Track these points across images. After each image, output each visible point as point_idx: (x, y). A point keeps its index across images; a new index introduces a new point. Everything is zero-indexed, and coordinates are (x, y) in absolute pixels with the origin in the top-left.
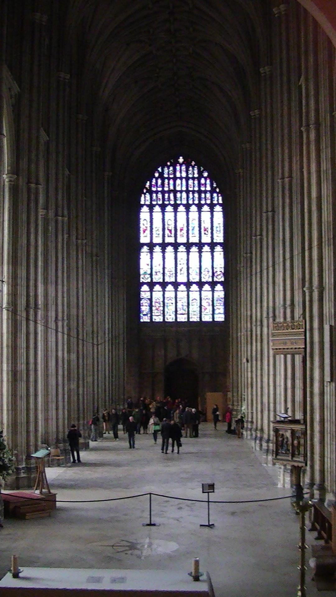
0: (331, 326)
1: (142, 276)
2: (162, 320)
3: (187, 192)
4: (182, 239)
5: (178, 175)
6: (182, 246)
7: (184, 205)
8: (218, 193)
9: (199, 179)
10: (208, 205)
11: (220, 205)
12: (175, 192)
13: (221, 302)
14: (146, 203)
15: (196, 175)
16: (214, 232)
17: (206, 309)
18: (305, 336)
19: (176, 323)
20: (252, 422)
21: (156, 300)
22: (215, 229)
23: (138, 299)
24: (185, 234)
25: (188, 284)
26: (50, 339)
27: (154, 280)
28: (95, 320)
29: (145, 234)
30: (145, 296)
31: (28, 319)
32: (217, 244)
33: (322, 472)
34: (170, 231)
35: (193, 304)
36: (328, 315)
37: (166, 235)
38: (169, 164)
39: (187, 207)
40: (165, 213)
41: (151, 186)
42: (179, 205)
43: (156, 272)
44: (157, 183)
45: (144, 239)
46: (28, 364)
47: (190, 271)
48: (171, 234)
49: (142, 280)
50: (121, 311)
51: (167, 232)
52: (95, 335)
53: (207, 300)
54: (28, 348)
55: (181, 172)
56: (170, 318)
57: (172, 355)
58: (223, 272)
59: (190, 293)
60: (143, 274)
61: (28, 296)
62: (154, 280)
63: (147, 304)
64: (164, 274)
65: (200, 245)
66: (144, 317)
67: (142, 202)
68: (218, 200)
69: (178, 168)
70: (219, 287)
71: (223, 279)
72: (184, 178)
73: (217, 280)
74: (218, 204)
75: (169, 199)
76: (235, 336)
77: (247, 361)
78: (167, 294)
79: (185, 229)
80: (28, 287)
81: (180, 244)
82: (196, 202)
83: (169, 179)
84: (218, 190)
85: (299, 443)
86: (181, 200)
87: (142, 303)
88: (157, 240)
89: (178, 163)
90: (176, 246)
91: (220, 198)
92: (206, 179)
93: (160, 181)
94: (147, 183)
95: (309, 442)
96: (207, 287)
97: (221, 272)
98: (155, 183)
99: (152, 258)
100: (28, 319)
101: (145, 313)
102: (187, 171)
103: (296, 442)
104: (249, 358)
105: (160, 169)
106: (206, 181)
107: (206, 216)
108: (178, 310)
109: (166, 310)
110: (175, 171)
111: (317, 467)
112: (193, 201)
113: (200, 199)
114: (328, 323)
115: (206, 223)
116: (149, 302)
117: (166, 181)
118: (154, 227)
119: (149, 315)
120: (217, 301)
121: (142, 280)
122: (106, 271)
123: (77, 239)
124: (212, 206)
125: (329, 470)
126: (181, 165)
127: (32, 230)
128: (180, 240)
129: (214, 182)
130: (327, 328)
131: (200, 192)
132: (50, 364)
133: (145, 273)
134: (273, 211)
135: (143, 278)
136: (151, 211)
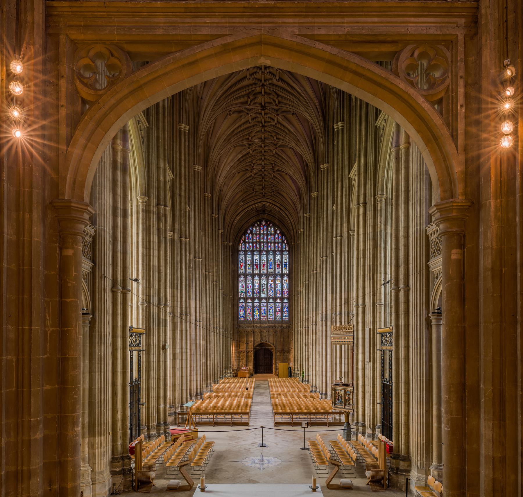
0: (370, 329)
3: (267, 243)
4: (264, 272)
5: (262, 232)
6: (264, 276)
8: (285, 244)
9: (274, 235)
11: (287, 251)
12: (260, 243)
15: (273, 233)
17: (278, 313)
18: (354, 334)
20: (308, 381)
25: (267, 299)
26: (192, 333)
28: (215, 321)
29: (242, 269)
31: (181, 322)
33: (364, 415)
34: (257, 267)
36: (368, 322)
38: (256, 225)
39: (267, 252)
41: (245, 239)
44: (249, 237)
45: (241, 271)
46: (182, 348)
49: (240, 296)
50: (228, 315)
51: (255, 267)
52: (215, 329)
54: (182, 339)
55: (263, 231)
57: (258, 341)
61: (181, 308)
64: (253, 292)
65: (275, 276)
69: (262, 228)
70: (286, 301)
75: (256, 248)
76: (296, 329)
77: (306, 345)
78: (255, 304)
79: (266, 265)
80: (181, 302)
81: (262, 275)
83: (256, 234)
84: (285, 242)
85: (349, 398)
86: (263, 248)
88: (249, 272)
89: (262, 224)
90: (260, 276)
92: (278, 235)
95: (355, 398)
96: (278, 301)
98: (248, 238)
99: (246, 283)
100: (181, 322)
102: (267, 230)
103: (347, 397)
104: (307, 344)
105: (251, 228)
106: (278, 236)
107: (278, 257)
110: (260, 229)
111: (360, 413)
112: (271, 248)
113: (275, 247)
114: (368, 327)
115: (278, 261)
121: (240, 296)
122: (221, 291)
123: (206, 272)
124: (282, 252)
125: (368, 415)
126: (263, 226)
127: (184, 267)
130: (367, 330)
131: (275, 243)
132: (192, 348)
134: (327, 256)
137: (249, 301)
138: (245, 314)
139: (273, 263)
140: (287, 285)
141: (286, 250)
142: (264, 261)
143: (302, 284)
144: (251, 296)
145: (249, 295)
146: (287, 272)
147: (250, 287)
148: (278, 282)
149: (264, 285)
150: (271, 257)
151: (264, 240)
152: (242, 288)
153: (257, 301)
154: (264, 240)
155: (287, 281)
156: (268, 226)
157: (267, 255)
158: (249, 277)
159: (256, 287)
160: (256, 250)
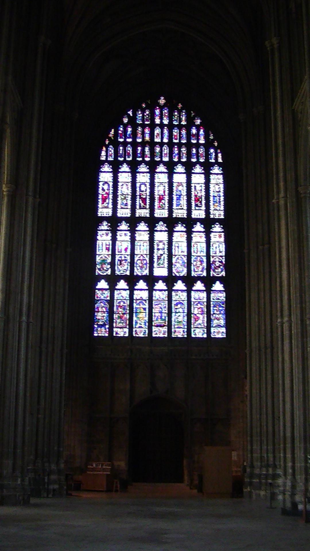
1: (98, 266)
2: (127, 335)
3: (171, 145)
4: (161, 213)
5: (158, 121)
6: (161, 223)
7: (165, 164)
9: (188, 128)
10: (201, 164)
11: (219, 165)
12: (152, 144)
13: (221, 308)
14: (109, 159)
15: (184, 123)
16: (211, 203)
17: (198, 318)
19: (150, 339)
21: (119, 303)
22: (211, 199)
23: (92, 301)
24: (167, 205)
27: (117, 273)
29: (105, 204)
30: (102, 297)
32: (215, 221)
34: (144, 200)
35: (178, 311)
37: (138, 207)
40: (138, 174)
41: (116, 134)
42: (158, 163)
44: (125, 131)
47: (174, 260)
48: (145, 204)
51: (138, 201)
53: (199, 306)
55: (161, 119)
56: (141, 332)
58: (224, 261)
59: (173, 294)
60: (101, 263)
62: (117, 273)
63: (104, 310)
66: (99, 329)
67: (103, 158)
68: (216, 158)
69: (157, 112)
70: (218, 286)
71: (223, 273)
72: (166, 125)
73: (215, 275)
74: (217, 163)
75: (143, 155)
78: (137, 295)
79: (167, 198)
82: (184, 160)
83: (144, 126)
84: (216, 144)
86: (161, 157)
87: (98, 308)
88: (124, 212)
89: (158, 104)
91: (220, 155)
92: (198, 128)
93: (130, 130)
94: (111, 131)
96: (199, 285)
97: (221, 262)
99: (114, 239)
101: (101, 323)
105: (130, 113)
106: (198, 131)
107: (198, 179)
108: (154, 319)
109: (135, 318)
110: (152, 116)
112: (180, 158)
113: (189, 155)
115: (199, 190)
116: (108, 306)
117: (140, 129)
118: (119, 193)
119: (107, 326)
120: (214, 306)
126: (162, 108)
128: (158, 213)
129: (210, 133)
131: (189, 146)
133: (103, 262)
135: (99, 269)
136: (116, 173)
137: (122, 284)
138: (111, 320)
139: (184, 193)
140: (223, 247)
141: (217, 163)
142: (161, 188)
143: (282, 184)
144: (128, 273)
145: (123, 269)
146: (220, 215)
147: (126, 250)
148: (199, 238)
149: (161, 246)
150: (180, 178)
151: (162, 138)
152: (105, 252)
153: (142, 284)
155: (220, 236)
156: (171, 107)
157: (171, 174)
158: (124, 226)
159: (142, 249)
160: (143, 161)
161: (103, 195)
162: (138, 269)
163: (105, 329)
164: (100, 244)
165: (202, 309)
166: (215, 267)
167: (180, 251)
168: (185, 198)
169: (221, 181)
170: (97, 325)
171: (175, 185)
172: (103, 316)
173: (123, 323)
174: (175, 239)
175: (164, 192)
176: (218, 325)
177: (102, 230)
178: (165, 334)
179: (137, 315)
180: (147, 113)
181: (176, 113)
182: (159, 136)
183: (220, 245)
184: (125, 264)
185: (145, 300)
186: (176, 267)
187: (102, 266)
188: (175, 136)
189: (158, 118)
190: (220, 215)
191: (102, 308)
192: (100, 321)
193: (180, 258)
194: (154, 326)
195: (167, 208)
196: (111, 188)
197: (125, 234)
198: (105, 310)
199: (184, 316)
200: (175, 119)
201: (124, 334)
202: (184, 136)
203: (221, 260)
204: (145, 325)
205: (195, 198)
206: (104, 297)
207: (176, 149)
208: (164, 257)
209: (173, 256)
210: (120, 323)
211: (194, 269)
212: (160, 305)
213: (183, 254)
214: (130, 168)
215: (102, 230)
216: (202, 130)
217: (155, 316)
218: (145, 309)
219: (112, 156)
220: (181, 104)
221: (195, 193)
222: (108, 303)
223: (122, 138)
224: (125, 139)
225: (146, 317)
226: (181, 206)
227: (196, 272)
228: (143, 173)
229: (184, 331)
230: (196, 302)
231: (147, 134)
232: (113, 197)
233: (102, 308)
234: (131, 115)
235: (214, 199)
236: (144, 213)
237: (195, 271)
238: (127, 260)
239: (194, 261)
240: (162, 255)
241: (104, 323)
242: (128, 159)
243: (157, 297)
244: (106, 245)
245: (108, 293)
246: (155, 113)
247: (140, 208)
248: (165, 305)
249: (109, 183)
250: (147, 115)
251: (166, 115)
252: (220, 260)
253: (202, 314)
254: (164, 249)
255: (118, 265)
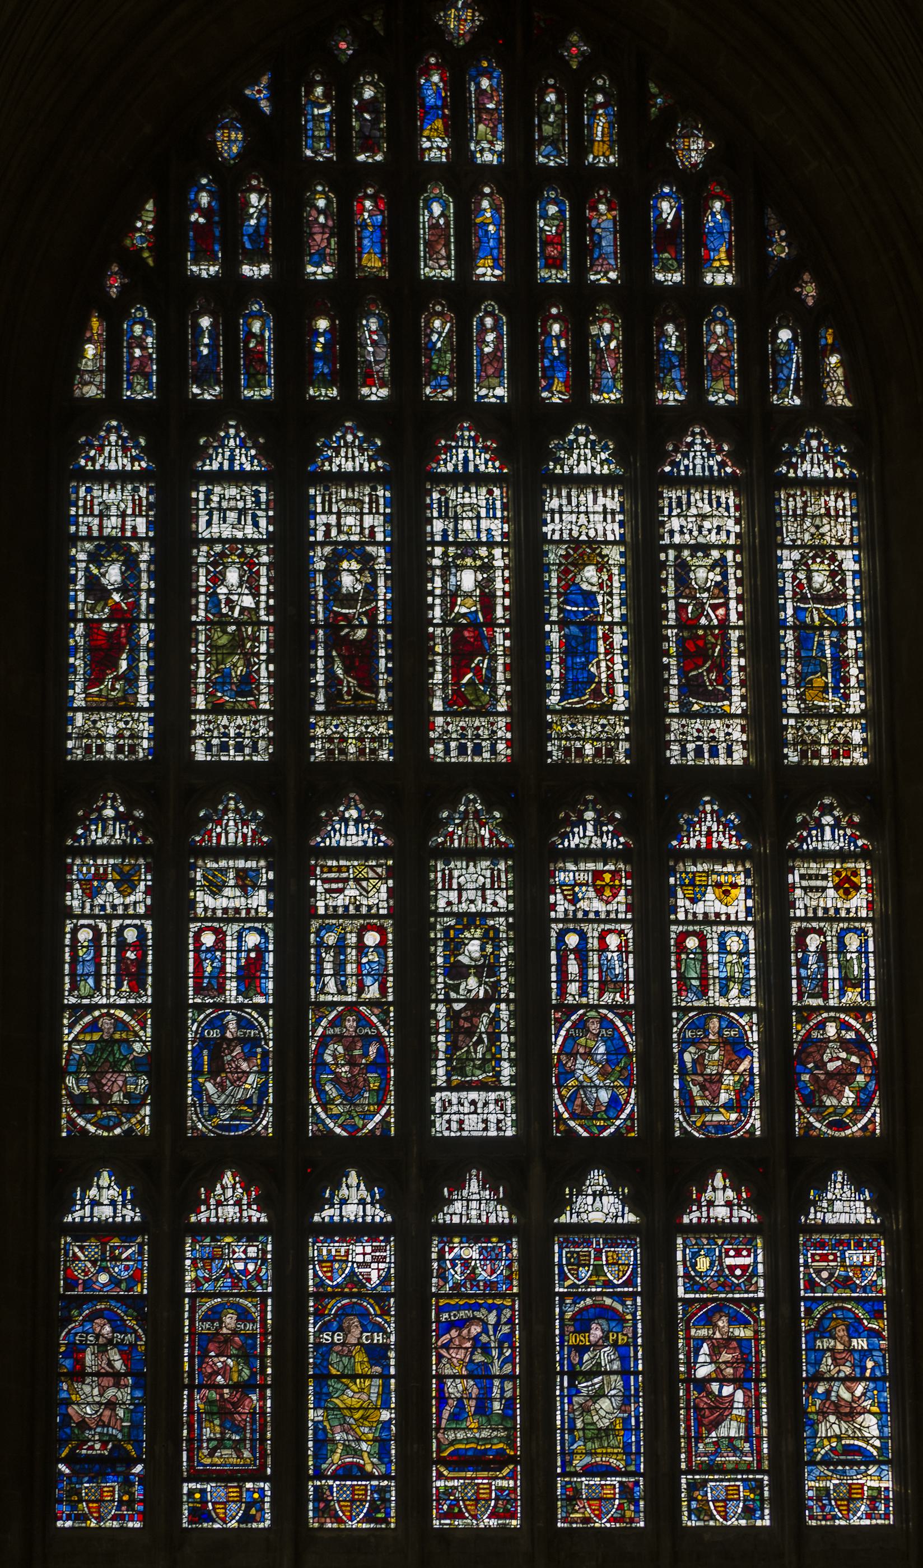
13: (860, 1343)
27: (198, 1123)
29: (111, 687)
43: (217, 1048)
59: (559, 1254)
62: (198, 1123)
84: (810, 291)
86: (463, 379)
87: (76, 1351)
97: (860, 1045)
116: (137, 1336)
120: (821, 1330)
135: (81, 1104)
142: (468, 580)
151: (466, 260)
154: (466, 260)
161: (91, 626)
162: (325, 1103)
163: (127, 1484)
164: (85, 935)
165: (740, 1346)
166: (815, 1078)
167: (593, 974)
168: (618, 640)
169: (843, 530)
170: (67, 1461)
171: (553, 556)
172: (111, 1405)
173: (237, 1447)
174: (561, 905)
175: (487, 601)
176: (849, 1450)
177: (96, 851)
178: (513, 1516)
179: (329, 1395)
180: (368, 93)
181: (551, 97)
182: (447, 246)
183: (853, 942)
184: (244, 1066)
185: (380, 1298)
186: (571, 1083)
187: (96, 1080)
188: (547, 242)
189: (439, 124)
190: (842, 746)
191: (102, 1349)
192: (87, 1434)
193: (594, 1027)
194: (442, 1461)
195: (502, 706)
196: (146, 583)
197: (242, 875)
198: (118, 1365)
199: (626, 1399)
200: (547, 130)
201: (246, 1518)
202: (607, 243)
203: (857, 1031)
204: (383, 1453)
205: (680, 641)
206: (115, 1281)
207: (556, 328)
208: (495, 1020)
209: (555, 1015)
210: (221, 1443)
211: (685, 1093)
212: (476, 1329)
213: (607, 998)
214: (263, 452)
215: (96, 851)
216: (717, 205)
217: (443, 1400)
218: (376, 1354)
219: (147, 376)
220: (586, 39)
221: (680, 608)
222: (141, 1320)
223: (212, 259)
224: (230, 266)
225: (386, 1406)
226: (597, 694)
227: (703, 1110)
228: (350, 479)
229: (626, 1491)
230: (705, 1302)
231: (366, 233)
232: (153, 635)
233: (102, 1349)
234: (265, 106)
235: (801, 642)
236: (361, 739)
237: (689, 1106)
238: (256, 1042)
239: (685, 1044)
240: (476, 1006)
241: (118, 1446)
242: (247, 393)
243: (457, 1275)
244: (122, 945)
245: (141, 1252)
246: (415, 93)
247: (334, 709)
248: (506, 1329)
249: (135, 546)
250: (366, 106)
251: (491, 106)
252: (851, 1035)
253: (738, 1382)
254: (492, 969)
255: (198, 1072)
